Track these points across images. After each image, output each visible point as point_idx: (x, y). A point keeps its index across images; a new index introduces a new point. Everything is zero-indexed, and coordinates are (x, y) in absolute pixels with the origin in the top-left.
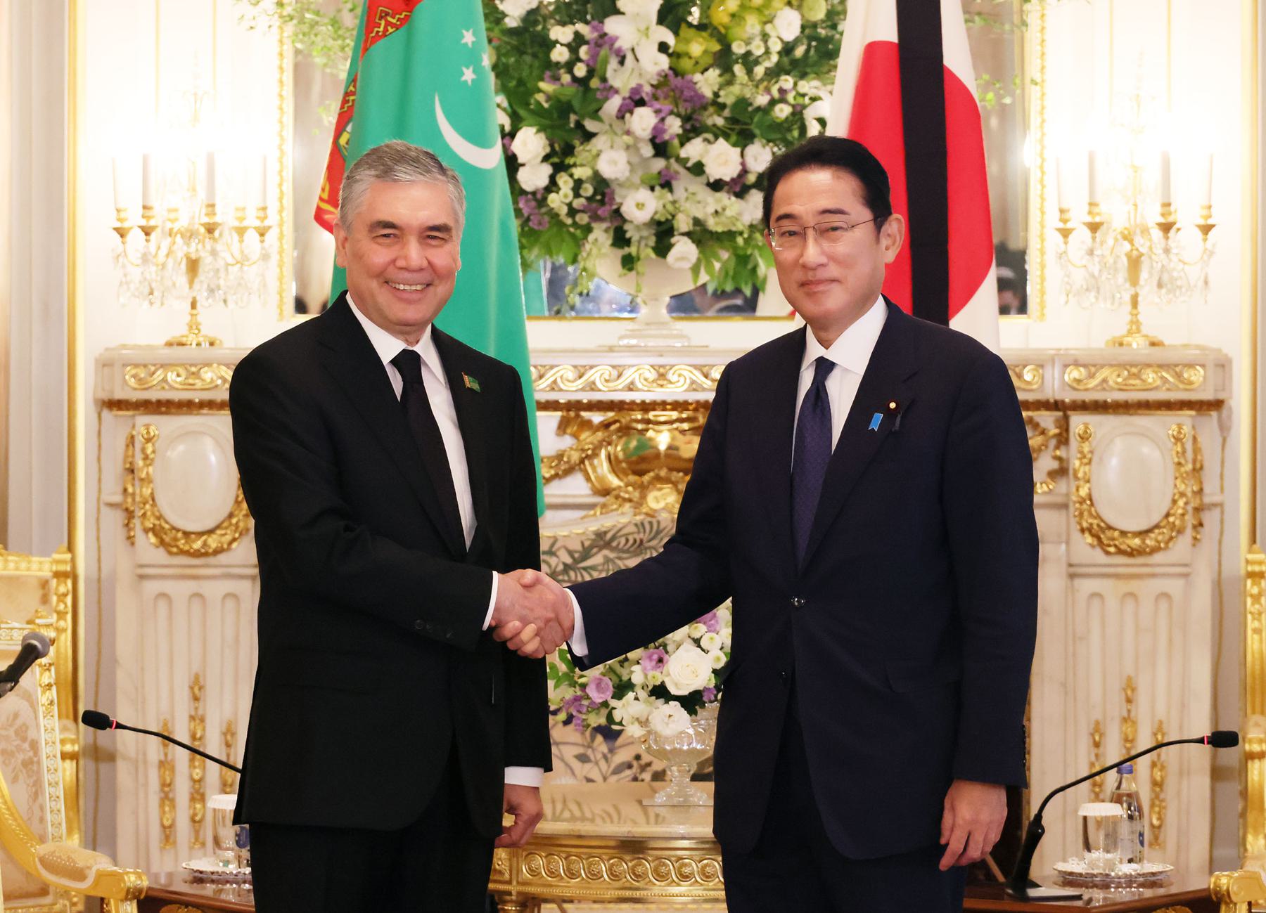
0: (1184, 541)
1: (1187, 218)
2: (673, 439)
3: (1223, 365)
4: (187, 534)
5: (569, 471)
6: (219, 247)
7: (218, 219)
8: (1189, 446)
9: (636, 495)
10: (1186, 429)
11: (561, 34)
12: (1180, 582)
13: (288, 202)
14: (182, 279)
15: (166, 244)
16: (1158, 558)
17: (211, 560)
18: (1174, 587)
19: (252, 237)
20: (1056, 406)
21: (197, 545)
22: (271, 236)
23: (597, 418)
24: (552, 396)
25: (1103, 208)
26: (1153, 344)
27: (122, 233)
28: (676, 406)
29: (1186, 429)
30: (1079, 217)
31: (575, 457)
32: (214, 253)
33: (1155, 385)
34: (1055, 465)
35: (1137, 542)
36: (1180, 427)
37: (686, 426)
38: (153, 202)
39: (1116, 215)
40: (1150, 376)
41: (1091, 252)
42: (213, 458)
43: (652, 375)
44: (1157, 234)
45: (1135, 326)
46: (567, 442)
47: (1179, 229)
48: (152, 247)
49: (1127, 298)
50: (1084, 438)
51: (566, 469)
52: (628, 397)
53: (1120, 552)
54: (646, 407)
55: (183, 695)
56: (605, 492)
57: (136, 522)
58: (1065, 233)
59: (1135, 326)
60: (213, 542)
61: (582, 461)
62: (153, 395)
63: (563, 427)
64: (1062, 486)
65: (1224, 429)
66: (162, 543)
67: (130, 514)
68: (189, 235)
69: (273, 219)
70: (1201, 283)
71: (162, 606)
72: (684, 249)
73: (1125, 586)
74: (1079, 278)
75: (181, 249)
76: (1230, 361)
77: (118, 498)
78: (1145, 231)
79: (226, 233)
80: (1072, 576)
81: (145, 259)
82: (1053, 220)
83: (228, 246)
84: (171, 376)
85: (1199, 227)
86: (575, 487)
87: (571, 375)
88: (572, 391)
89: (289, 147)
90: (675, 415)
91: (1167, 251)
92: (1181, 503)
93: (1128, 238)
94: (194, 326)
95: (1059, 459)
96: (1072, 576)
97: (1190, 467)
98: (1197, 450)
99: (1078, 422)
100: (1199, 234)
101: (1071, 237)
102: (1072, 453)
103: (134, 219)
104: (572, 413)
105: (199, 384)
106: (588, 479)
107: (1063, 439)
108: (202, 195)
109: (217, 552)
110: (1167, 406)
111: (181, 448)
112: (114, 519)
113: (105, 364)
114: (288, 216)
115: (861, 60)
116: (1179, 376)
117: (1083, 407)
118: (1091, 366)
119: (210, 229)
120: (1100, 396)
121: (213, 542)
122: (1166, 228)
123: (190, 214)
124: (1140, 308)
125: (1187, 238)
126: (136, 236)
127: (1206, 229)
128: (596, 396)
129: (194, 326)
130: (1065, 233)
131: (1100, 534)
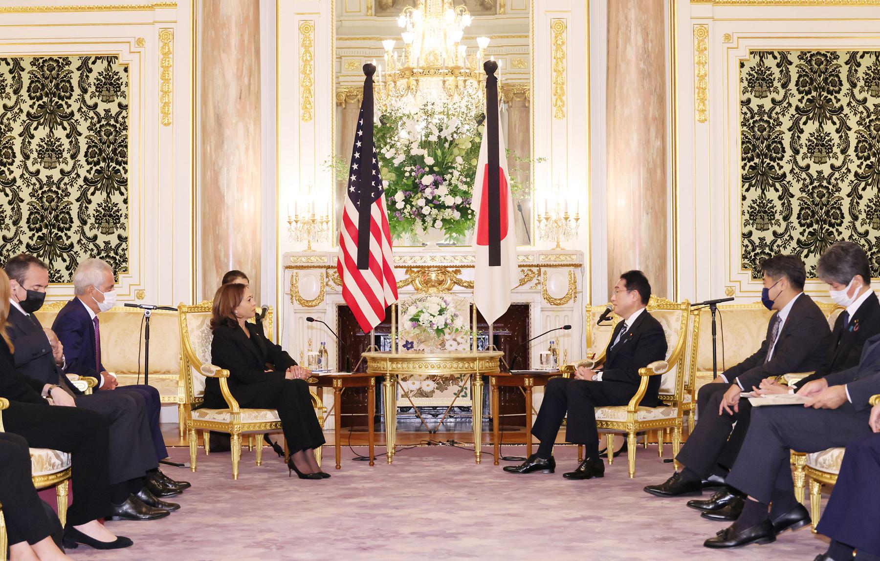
0: (572, 301)
1: (572, 216)
2: (437, 275)
3: (582, 255)
4: (307, 301)
5: (408, 284)
6: (316, 226)
7: (315, 218)
8: (573, 276)
9: (426, 289)
10: (572, 272)
11: (408, 169)
12: (570, 312)
13: (335, 216)
14: (305, 235)
15: (302, 225)
16: (564, 306)
17: (313, 308)
18: (569, 313)
19: (325, 224)
20: (538, 266)
21: (310, 304)
22: (330, 223)
23: (415, 270)
24: (404, 264)
25: (550, 214)
26: (563, 249)
27: (290, 223)
28: (436, 267)
29: (572, 272)
30: (543, 216)
31: (410, 280)
32: (314, 227)
33: (564, 260)
34: (537, 282)
35: (559, 302)
36: (570, 271)
37: (439, 272)
38: (298, 214)
39: (554, 217)
40: (561, 257)
41: (546, 225)
42: (315, 286)
43: (429, 259)
44: (564, 221)
45: (558, 246)
46: (408, 276)
47: (570, 221)
48: (298, 226)
49: (556, 238)
50: (545, 273)
51: (406, 283)
52: (424, 265)
53: (555, 304)
54: (429, 267)
55: (306, 344)
56: (417, 289)
57: (294, 298)
58: (540, 221)
59: (558, 246)
60: (314, 303)
61: (412, 282)
62: (298, 264)
63: (407, 272)
64: (539, 287)
65: (583, 273)
66: (301, 304)
67: (292, 296)
68: (308, 223)
69: (330, 218)
70: (576, 234)
71: (301, 319)
72: (439, 224)
73: (555, 314)
74: (543, 233)
75: (306, 227)
76: (584, 254)
77: (289, 292)
78: (560, 220)
79: (318, 224)
80: (542, 311)
81: (296, 228)
82: (536, 218)
83: (318, 226)
84: (304, 260)
85: (575, 219)
86: (410, 288)
87: (408, 258)
88: (410, 263)
89: (335, 202)
90: (436, 269)
91: (566, 225)
92: (571, 291)
93: (556, 222)
94: (309, 248)
95: (538, 280)
96: (542, 311)
97: (573, 282)
98: (575, 277)
99: (543, 269)
100: (575, 221)
101: (542, 222)
102: (541, 278)
103: (293, 218)
104: (409, 269)
105: (310, 261)
106: (414, 286)
107: (539, 274)
108: (311, 213)
109: (315, 306)
110: (567, 265)
111: (305, 279)
112: (288, 297)
113: (286, 256)
114: (335, 220)
115: (485, 172)
116: (570, 257)
117: (544, 266)
118: (547, 255)
119: (313, 221)
120: (549, 263)
121: (314, 303)
122: (566, 219)
123: (308, 217)
124: (560, 240)
125: (573, 223)
126: (294, 223)
127: (577, 219)
128: (415, 265)
129: (309, 248)
130: (540, 221)
131: (549, 299)
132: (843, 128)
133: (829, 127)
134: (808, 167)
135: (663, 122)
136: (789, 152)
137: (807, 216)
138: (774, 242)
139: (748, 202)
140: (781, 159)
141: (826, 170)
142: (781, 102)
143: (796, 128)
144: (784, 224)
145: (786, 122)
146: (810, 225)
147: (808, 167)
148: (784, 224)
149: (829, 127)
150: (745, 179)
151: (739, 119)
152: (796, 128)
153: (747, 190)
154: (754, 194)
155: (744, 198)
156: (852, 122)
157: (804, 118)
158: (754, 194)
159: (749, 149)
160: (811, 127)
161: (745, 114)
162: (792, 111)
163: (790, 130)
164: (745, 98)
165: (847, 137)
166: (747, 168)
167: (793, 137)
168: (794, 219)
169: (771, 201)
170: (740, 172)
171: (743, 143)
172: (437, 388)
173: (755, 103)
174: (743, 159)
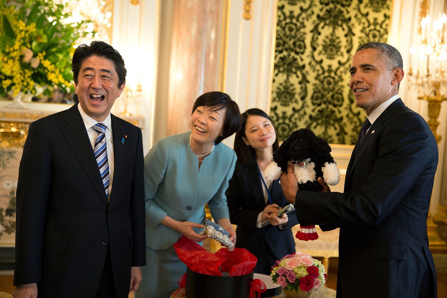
132: (350, 33)
133: (340, 33)
134: (321, 61)
135: (218, 16)
136: (309, 49)
137: (318, 98)
138: (292, 116)
139: (277, 84)
140: (303, 53)
141: (335, 65)
142: (306, 10)
143: (316, 31)
144: (301, 103)
145: (309, 26)
146: (319, 105)
147: (321, 61)
148: (301, 103)
149: (340, 33)
150: (276, 66)
151: (275, 21)
152: (316, 31)
153: (277, 75)
154: (282, 78)
155: (274, 81)
156: (357, 30)
157: (322, 24)
158: (282, 78)
159: (281, 44)
160: (326, 31)
161: (280, 17)
162: (314, 17)
163: (311, 32)
164: (280, 4)
165: (352, 41)
166: (278, 58)
167: (313, 38)
168: (308, 99)
169: (292, 85)
170: (273, 62)
171: (277, 39)
172: (5, 231)
173: (288, 9)
174: (276, 51)
